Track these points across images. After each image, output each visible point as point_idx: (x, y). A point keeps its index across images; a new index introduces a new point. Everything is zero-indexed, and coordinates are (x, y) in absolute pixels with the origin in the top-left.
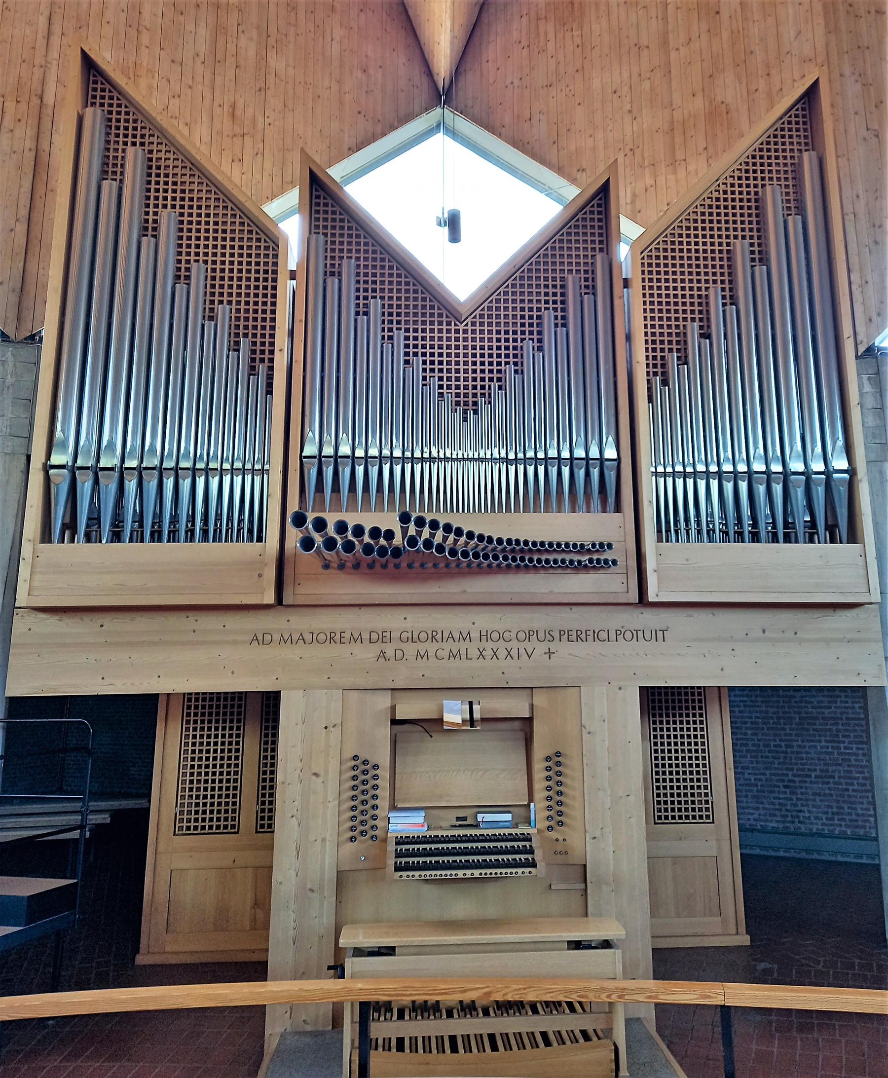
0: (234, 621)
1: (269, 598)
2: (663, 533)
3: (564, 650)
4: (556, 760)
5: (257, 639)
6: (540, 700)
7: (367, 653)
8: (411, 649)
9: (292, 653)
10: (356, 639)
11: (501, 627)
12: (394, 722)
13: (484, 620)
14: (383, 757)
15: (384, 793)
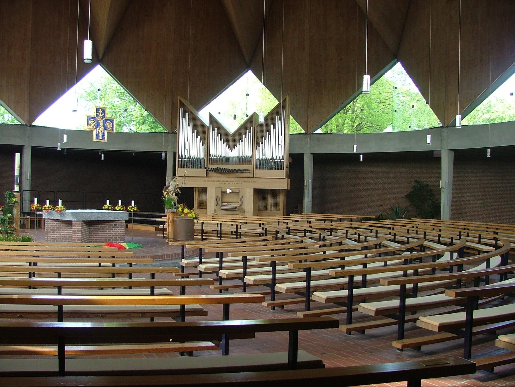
0: (202, 178)
1: (205, 176)
2: (256, 168)
3: (244, 183)
4: (242, 197)
5: (205, 181)
6: (240, 190)
7: (218, 183)
8: (224, 183)
9: (209, 183)
10: (217, 181)
11: (235, 180)
12: (222, 192)
13: (233, 179)
14: (220, 196)
15: (220, 201)
